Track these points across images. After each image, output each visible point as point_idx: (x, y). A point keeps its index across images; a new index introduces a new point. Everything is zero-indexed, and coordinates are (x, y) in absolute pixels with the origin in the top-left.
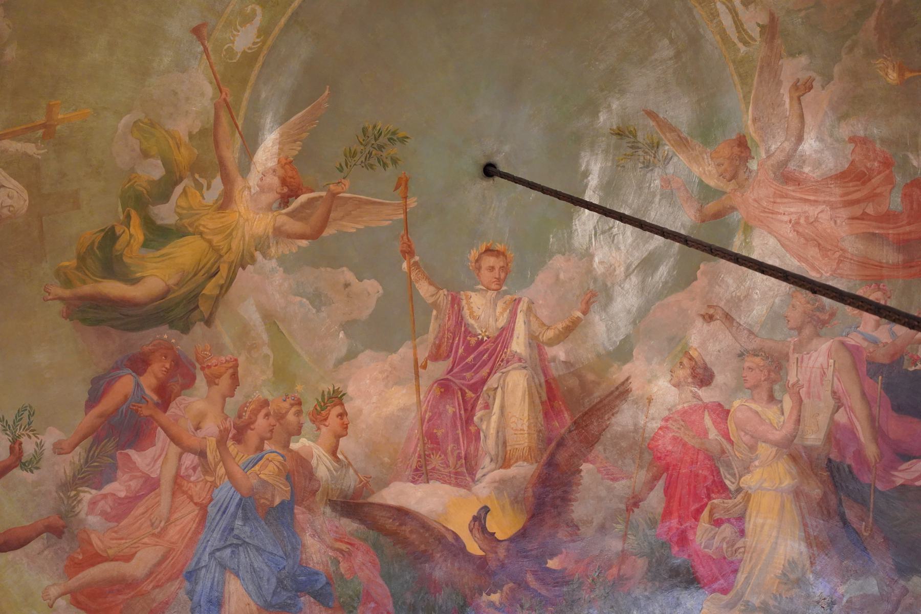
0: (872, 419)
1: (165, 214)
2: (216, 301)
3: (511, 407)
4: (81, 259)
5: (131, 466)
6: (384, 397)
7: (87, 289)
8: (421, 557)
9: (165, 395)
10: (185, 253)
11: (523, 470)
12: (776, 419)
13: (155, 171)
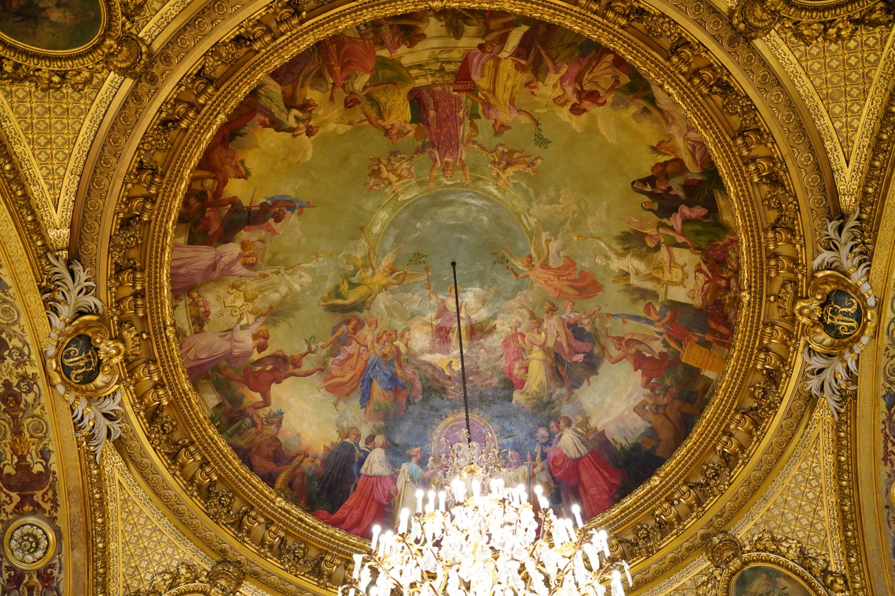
0: (568, 340)
2: (371, 303)
4: (329, 294)
5: (345, 351)
7: (331, 302)
9: (355, 330)
10: (362, 290)
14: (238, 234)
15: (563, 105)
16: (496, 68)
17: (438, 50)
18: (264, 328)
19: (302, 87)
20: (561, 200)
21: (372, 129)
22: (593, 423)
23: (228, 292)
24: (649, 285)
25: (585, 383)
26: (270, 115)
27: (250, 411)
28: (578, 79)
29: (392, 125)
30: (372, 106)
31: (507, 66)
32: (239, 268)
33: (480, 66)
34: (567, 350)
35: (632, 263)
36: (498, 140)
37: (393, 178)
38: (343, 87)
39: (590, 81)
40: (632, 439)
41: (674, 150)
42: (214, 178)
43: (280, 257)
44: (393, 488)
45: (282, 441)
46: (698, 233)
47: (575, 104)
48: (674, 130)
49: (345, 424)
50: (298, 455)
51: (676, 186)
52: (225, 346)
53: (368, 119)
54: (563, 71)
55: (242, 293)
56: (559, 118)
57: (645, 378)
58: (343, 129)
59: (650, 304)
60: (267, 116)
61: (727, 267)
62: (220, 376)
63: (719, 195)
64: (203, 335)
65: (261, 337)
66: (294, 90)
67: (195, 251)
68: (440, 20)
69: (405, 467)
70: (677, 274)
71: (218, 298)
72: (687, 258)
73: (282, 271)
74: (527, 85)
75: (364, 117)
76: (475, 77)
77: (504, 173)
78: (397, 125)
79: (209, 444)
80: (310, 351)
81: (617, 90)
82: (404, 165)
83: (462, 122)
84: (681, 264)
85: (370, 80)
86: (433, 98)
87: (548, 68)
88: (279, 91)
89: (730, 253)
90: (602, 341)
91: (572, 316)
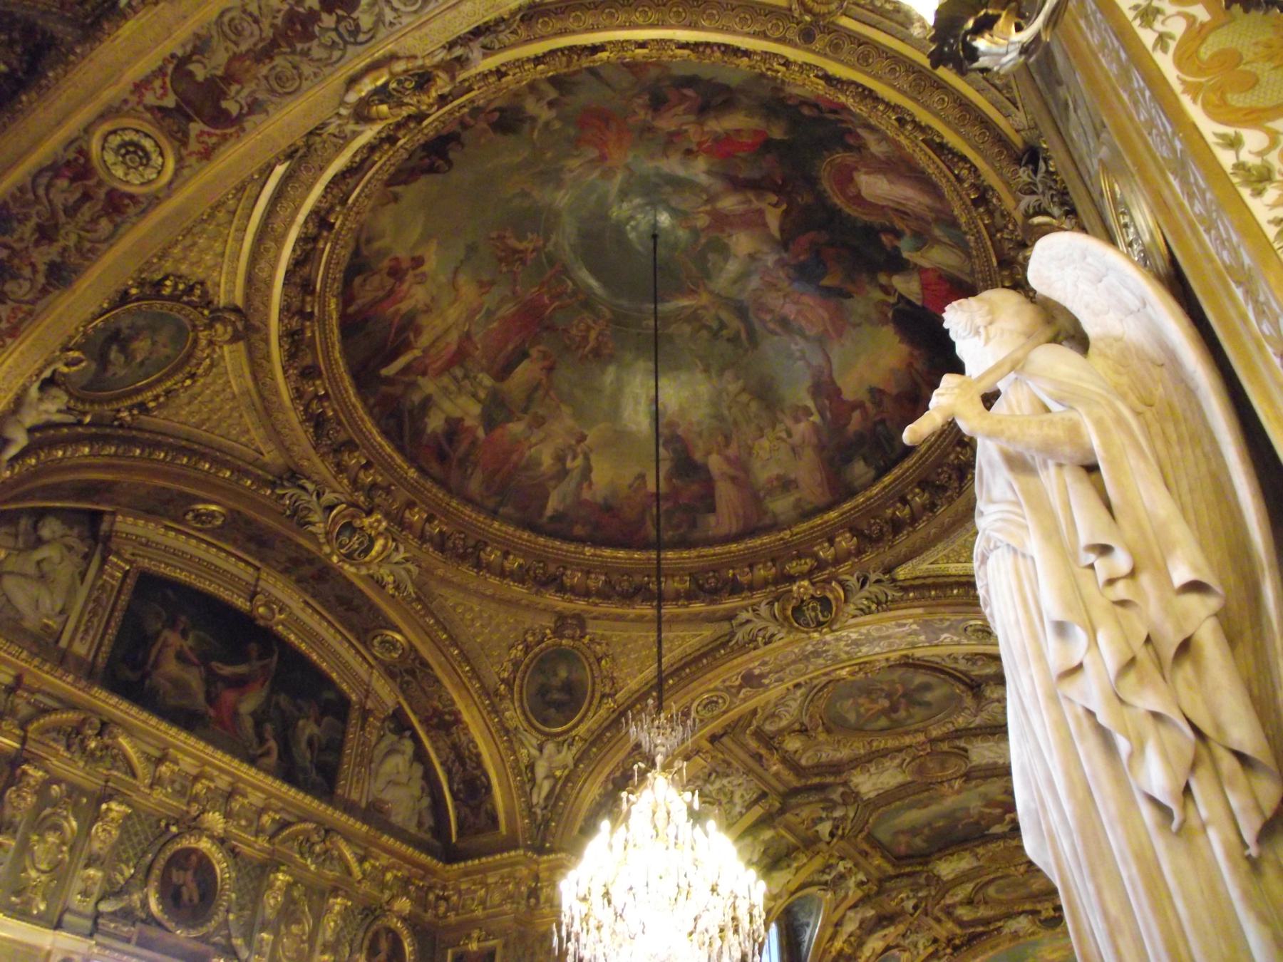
1: (715, 325)
13: (704, 333)
16: (433, 344)
26: (579, 485)
31: (425, 340)
32: (732, 451)
38: (527, 438)
53: (547, 394)
54: (392, 310)
76: (454, 347)
80: (803, 357)
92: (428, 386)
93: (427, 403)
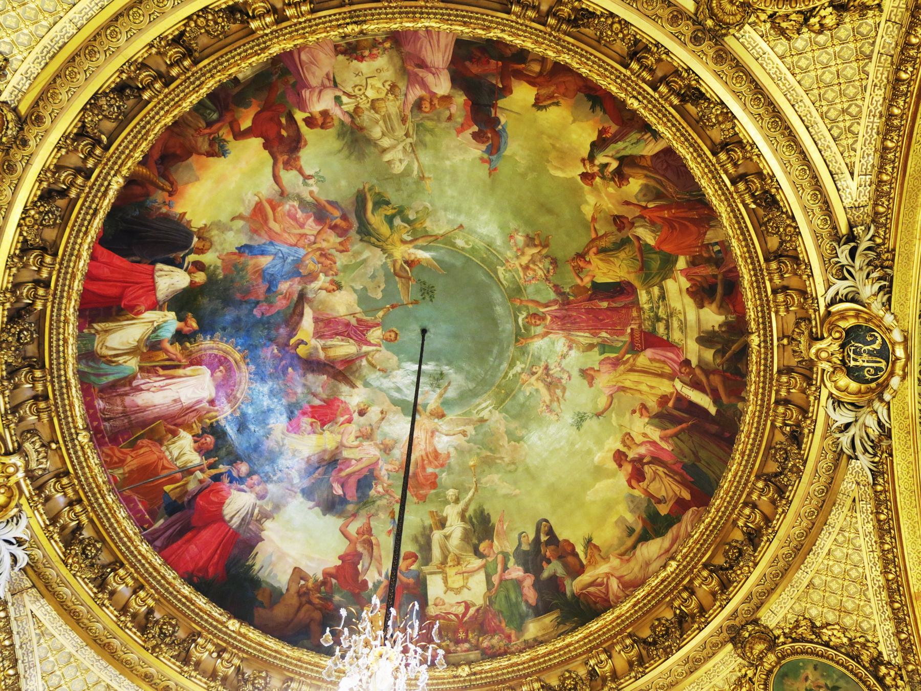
0: (354, 473)
1: (397, 221)
2: (369, 242)
3: (343, 348)
4: (379, 194)
5: (308, 218)
6: (343, 304)
7: (368, 197)
8: (287, 322)
9: (334, 228)
10: (385, 229)
11: (322, 355)
12: (350, 440)
13: (412, 216)
14: (461, 93)
15: (623, 442)
16: (661, 375)
17: (682, 318)
18: (336, 122)
19: (646, 176)
20: (513, 443)
21: (585, 241)
22: (268, 524)
23: (386, 81)
24: (436, 553)
25: (311, 504)
26: (615, 139)
27: (228, 118)
28: (655, 460)
29: (589, 262)
30: (614, 243)
31: (665, 387)
32: (416, 92)
33: (663, 358)
34: (343, 474)
35: (456, 528)
36: (575, 373)
37: (525, 260)
38: (641, 217)
39: (655, 473)
40: (263, 575)
41: (593, 563)
42: (540, 74)
43: (428, 138)
44: (143, 308)
45: (190, 160)
46: (507, 597)
47: (627, 456)
48: (615, 562)
49: (214, 232)
50: (172, 184)
51: (554, 568)
52: (314, 81)
53: (598, 238)
54: (664, 445)
55: (383, 95)
56: (608, 438)
57: (334, 571)
58: (588, 211)
59: (416, 557)
60: (614, 135)
61: (479, 637)
62: (274, 78)
63: (555, 616)
64: (332, 54)
65: (325, 120)
66: (643, 168)
67: (446, 46)
68: (720, 326)
69: (172, 315)
70: (456, 581)
71: (379, 70)
72: (476, 590)
73: (409, 140)
74: (644, 407)
75: (601, 233)
76: (649, 352)
77: (538, 379)
78: (589, 267)
79: (193, 83)
80: (307, 178)
81: (649, 501)
82: (540, 273)
83: (595, 335)
84: (469, 585)
85: (647, 244)
86: (623, 307)
87: (666, 429)
88: (644, 153)
89: (496, 637)
90: (363, 512)
91: (383, 472)
92: (693, 351)
93: (706, 339)
